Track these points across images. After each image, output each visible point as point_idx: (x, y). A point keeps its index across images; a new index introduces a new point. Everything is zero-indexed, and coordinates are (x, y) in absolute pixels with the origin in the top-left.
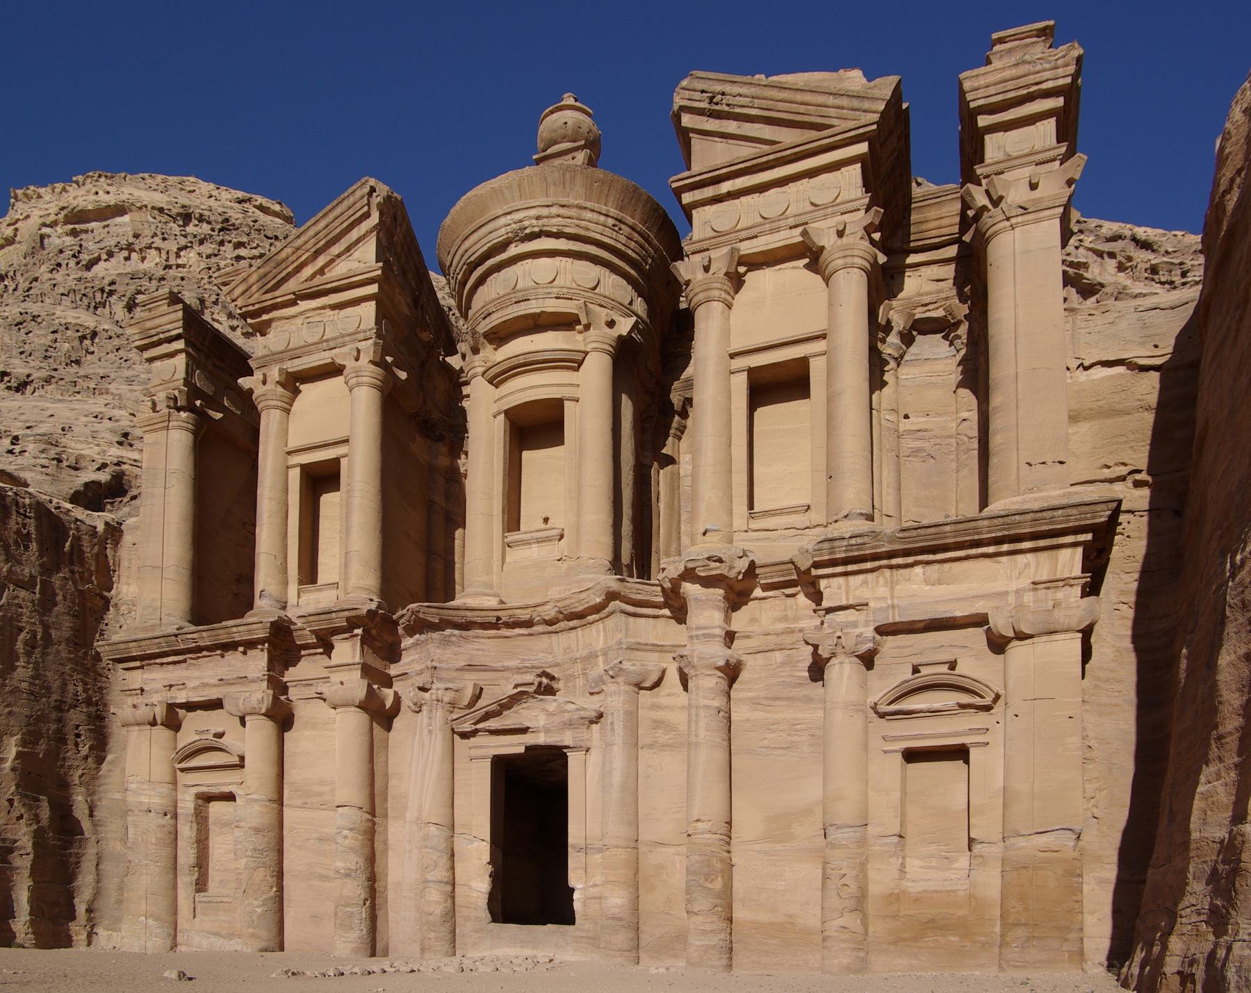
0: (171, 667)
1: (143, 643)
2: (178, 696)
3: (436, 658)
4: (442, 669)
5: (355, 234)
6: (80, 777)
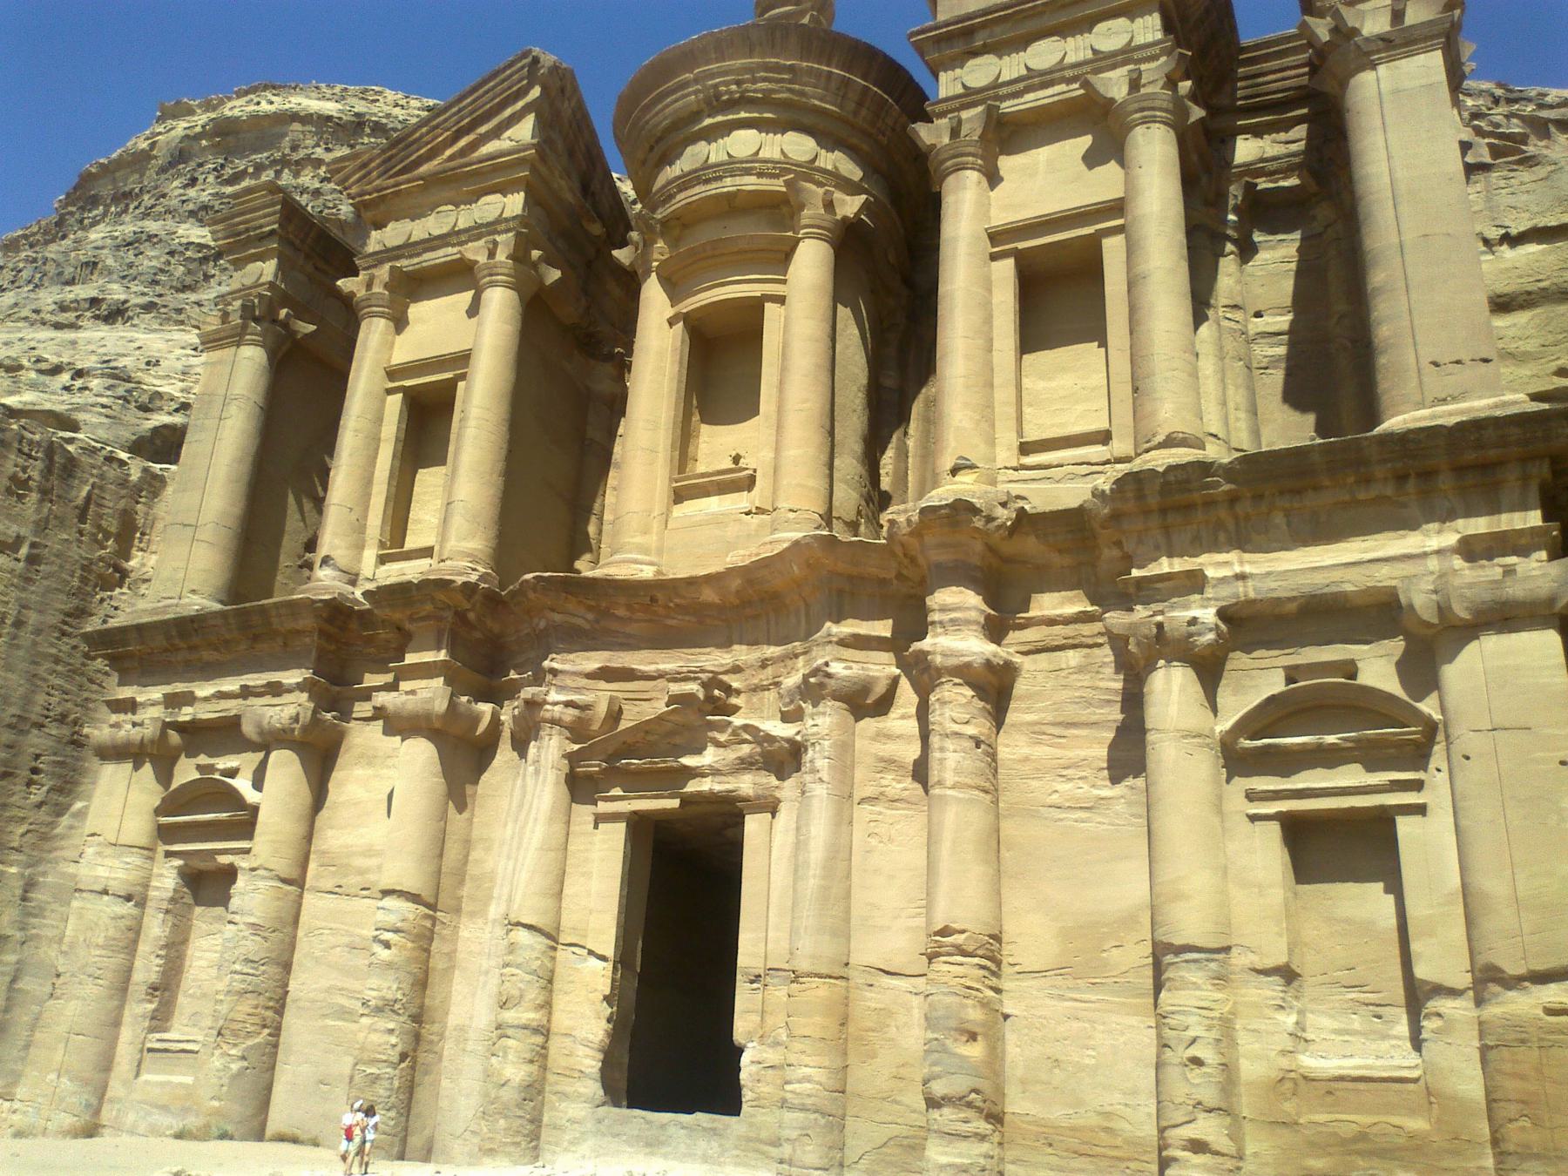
6: (23, 835)
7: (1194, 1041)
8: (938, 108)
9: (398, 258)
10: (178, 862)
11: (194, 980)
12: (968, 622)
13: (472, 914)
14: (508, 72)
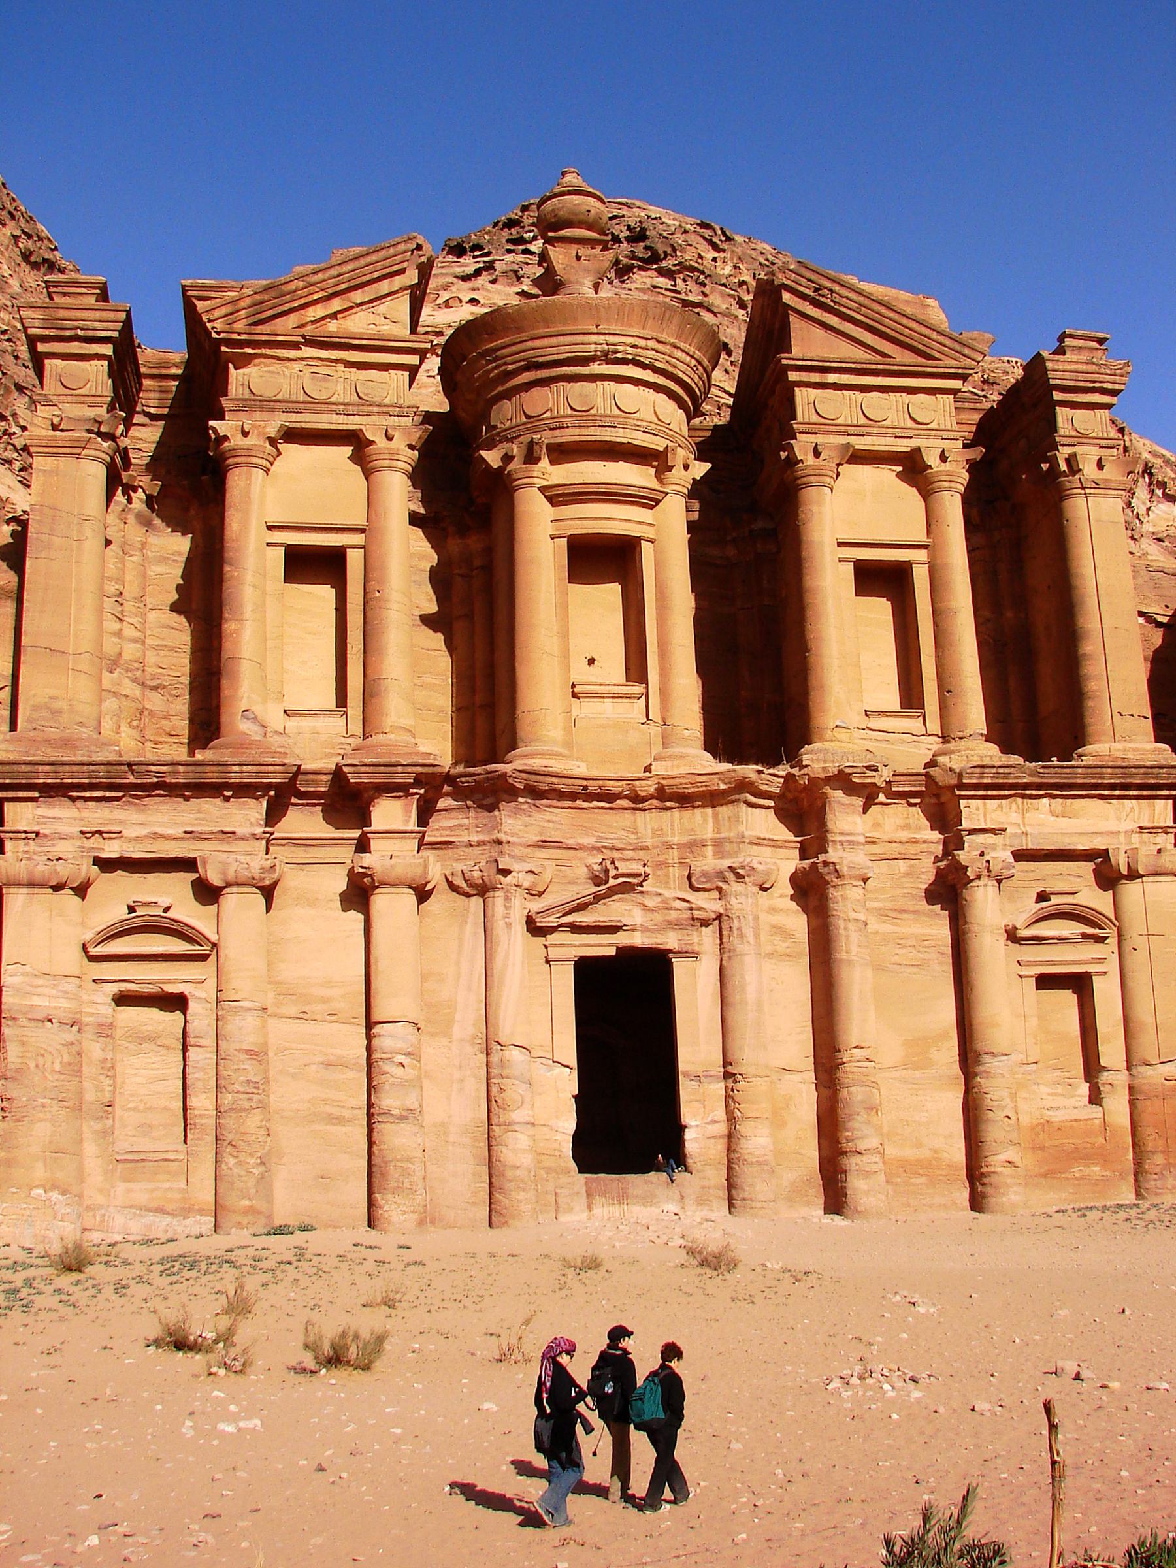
0: (91, 804)
1: (61, 768)
2: (106, 848)
3: (506, 829)
4: (514, 844)
7: (1003, 1108)
9: (273, 410)
10: (115, 988)
11: (132, 1095)
12: (859, 843)
13: (433, 1035)
14: (392, 251)
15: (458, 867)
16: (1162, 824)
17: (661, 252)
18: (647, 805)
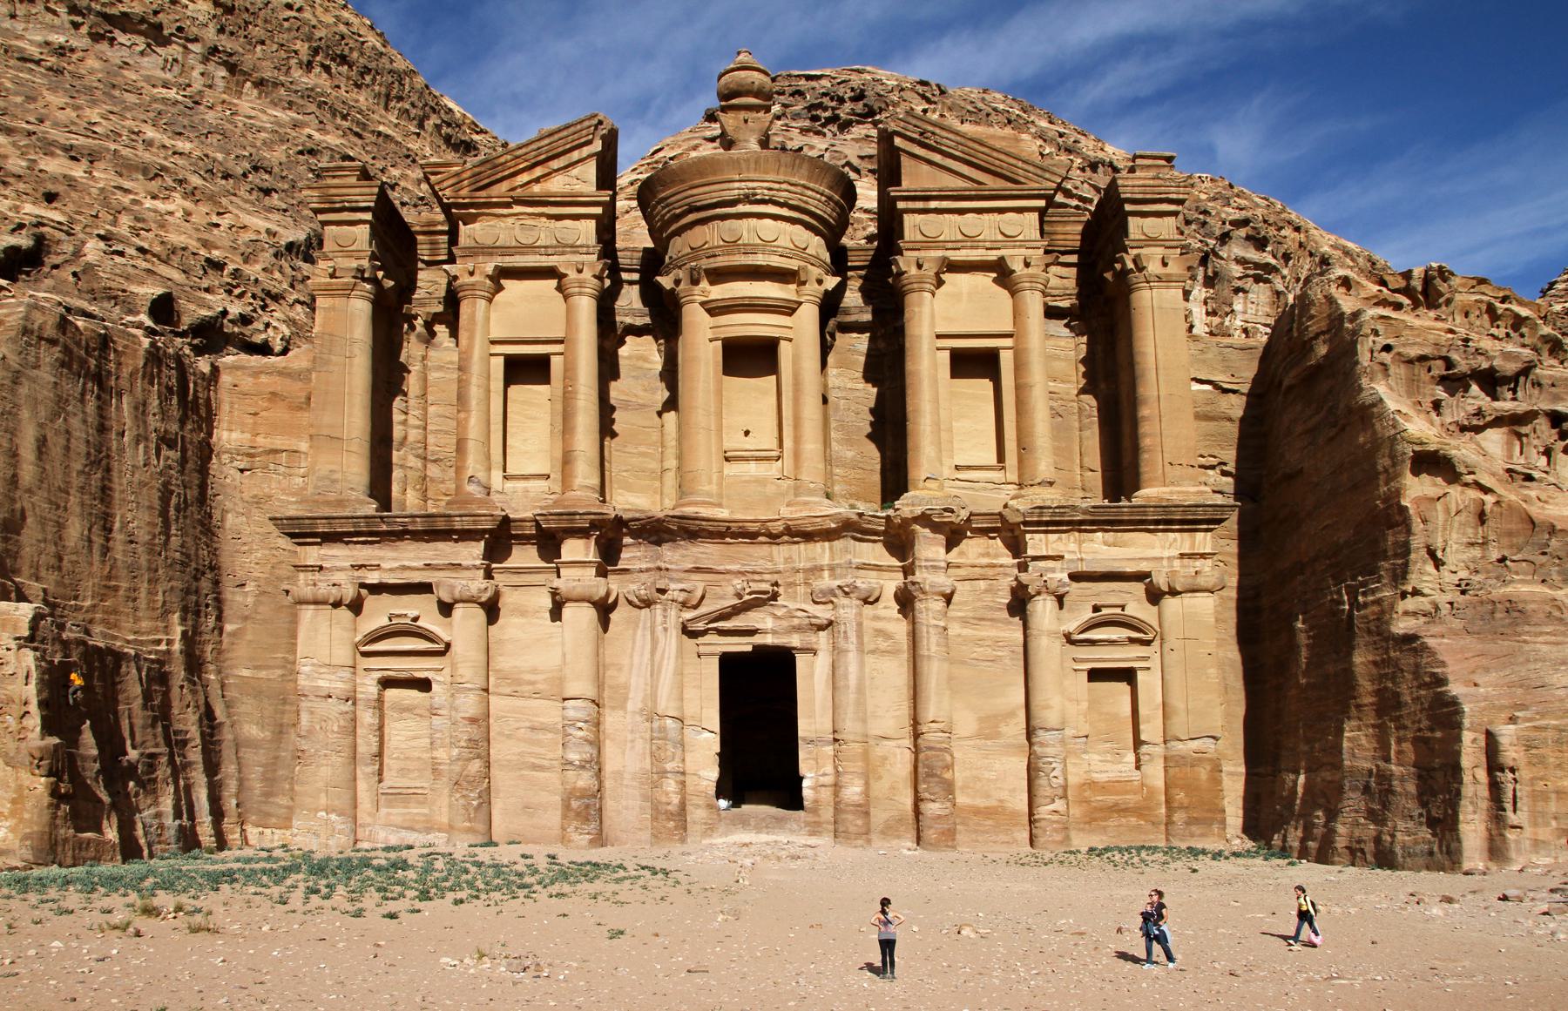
5: (575, 155)
8: (908, 245)
12: (940, 568)
15: (633, 587)
16: (1202, 551)
17: (876, 107)
18: (778, 541)
